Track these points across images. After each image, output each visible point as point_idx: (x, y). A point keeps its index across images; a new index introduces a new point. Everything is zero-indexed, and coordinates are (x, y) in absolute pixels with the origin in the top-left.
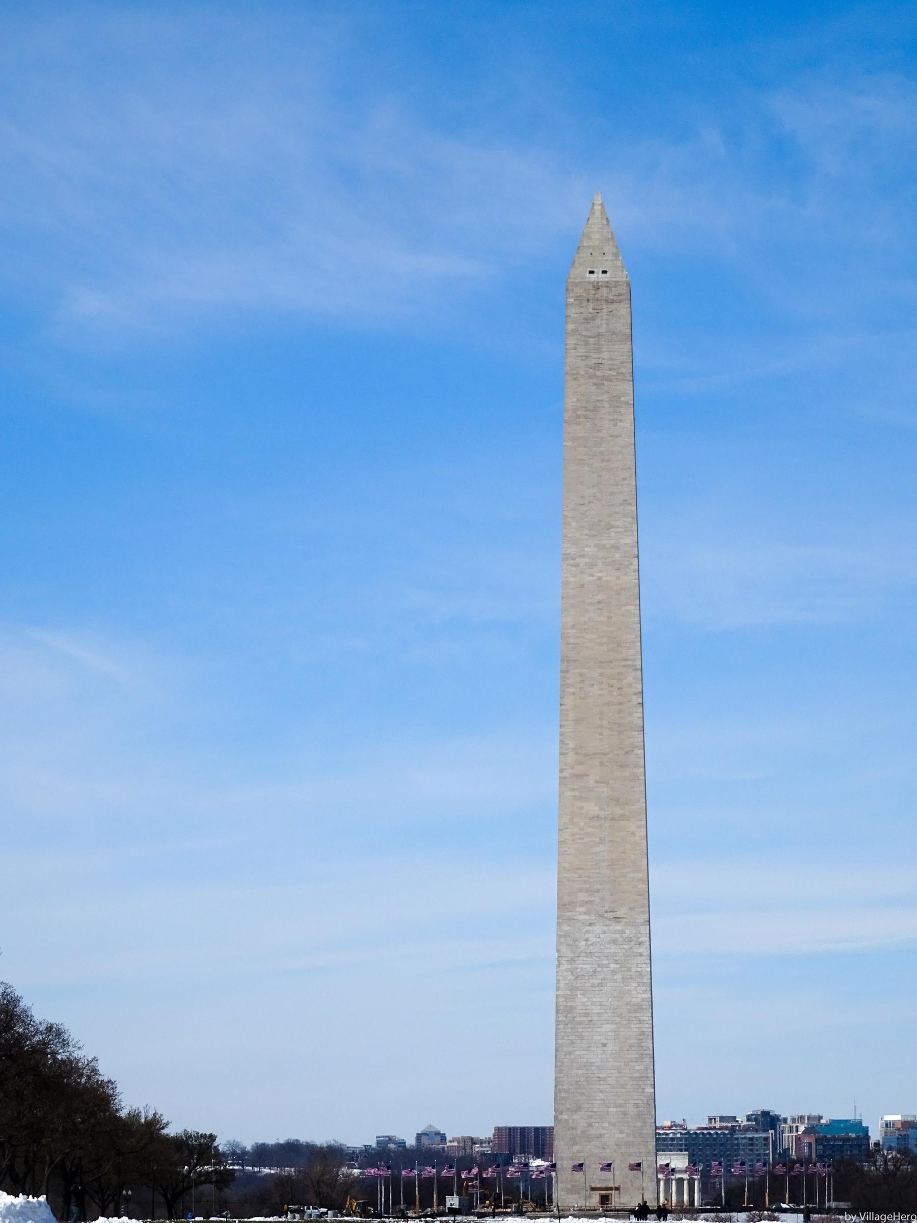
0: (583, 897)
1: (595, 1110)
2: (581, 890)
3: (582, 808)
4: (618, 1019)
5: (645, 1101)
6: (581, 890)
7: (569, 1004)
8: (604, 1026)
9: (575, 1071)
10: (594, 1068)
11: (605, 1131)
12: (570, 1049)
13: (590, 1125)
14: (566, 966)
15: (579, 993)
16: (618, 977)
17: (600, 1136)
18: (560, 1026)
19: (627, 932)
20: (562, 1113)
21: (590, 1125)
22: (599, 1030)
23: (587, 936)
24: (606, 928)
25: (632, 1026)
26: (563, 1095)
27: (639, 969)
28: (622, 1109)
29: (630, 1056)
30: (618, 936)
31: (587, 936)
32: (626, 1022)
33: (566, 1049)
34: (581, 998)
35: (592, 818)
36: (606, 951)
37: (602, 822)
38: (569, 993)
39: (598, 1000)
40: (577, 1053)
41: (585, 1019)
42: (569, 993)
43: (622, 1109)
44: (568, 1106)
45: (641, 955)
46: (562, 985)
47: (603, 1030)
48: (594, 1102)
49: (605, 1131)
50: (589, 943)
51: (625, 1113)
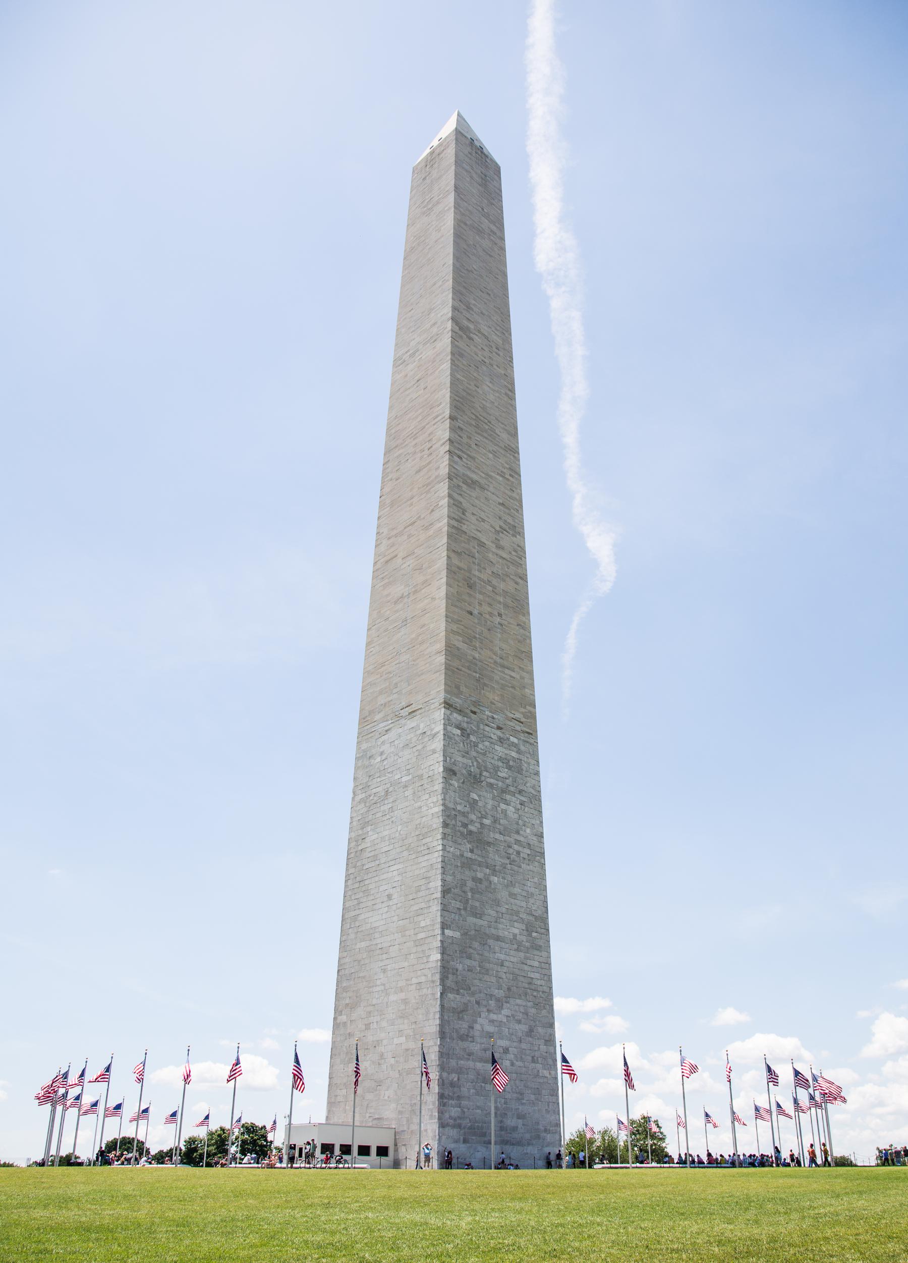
0: (382, 700)
1: (374, 1001)
2: (381, 692)
3: (388, 595)
4: (406, 853)
5: (430, 975)
6: (381, 692)
7: (360, 848)
8: (392, 869)
9: (358, 946)
10: (377, 935)
11: (383, 1035)
12: (357, 912)
13: (368, 1027)
14: (360, 797)
15: (369, 828)
16: (409, 793)
17: (378, 1043)
18: (350, 882)
19: (422, 726)
20: (341, 1013)
21: (368, 1027)
22: (385, 876)
23: (383, 748)
24: (400, 730)
25: (421, 859)
26: (344, 985)
27: (431, 773)
28: (402, 995)
29: (415, 908)
30: (412, 735)
31: (383, 748)
32: (414, 856)
33: (353, 914)
34: (372, 836)
35: (396, 603)
36: (400, 760)
37: (406, 600)
38: (360, 832)
39: (386, 833)
40: (362, 917)
41: (373, 864)
42: (360, 832)
43: (402, 995)
44: (347, 1001)
45: (434, 752)
46: (355, 823)
47: (390, 875)
48: (375, 989)
49: (383, 1035)
50: (384, 757)
51: (405, 1001)
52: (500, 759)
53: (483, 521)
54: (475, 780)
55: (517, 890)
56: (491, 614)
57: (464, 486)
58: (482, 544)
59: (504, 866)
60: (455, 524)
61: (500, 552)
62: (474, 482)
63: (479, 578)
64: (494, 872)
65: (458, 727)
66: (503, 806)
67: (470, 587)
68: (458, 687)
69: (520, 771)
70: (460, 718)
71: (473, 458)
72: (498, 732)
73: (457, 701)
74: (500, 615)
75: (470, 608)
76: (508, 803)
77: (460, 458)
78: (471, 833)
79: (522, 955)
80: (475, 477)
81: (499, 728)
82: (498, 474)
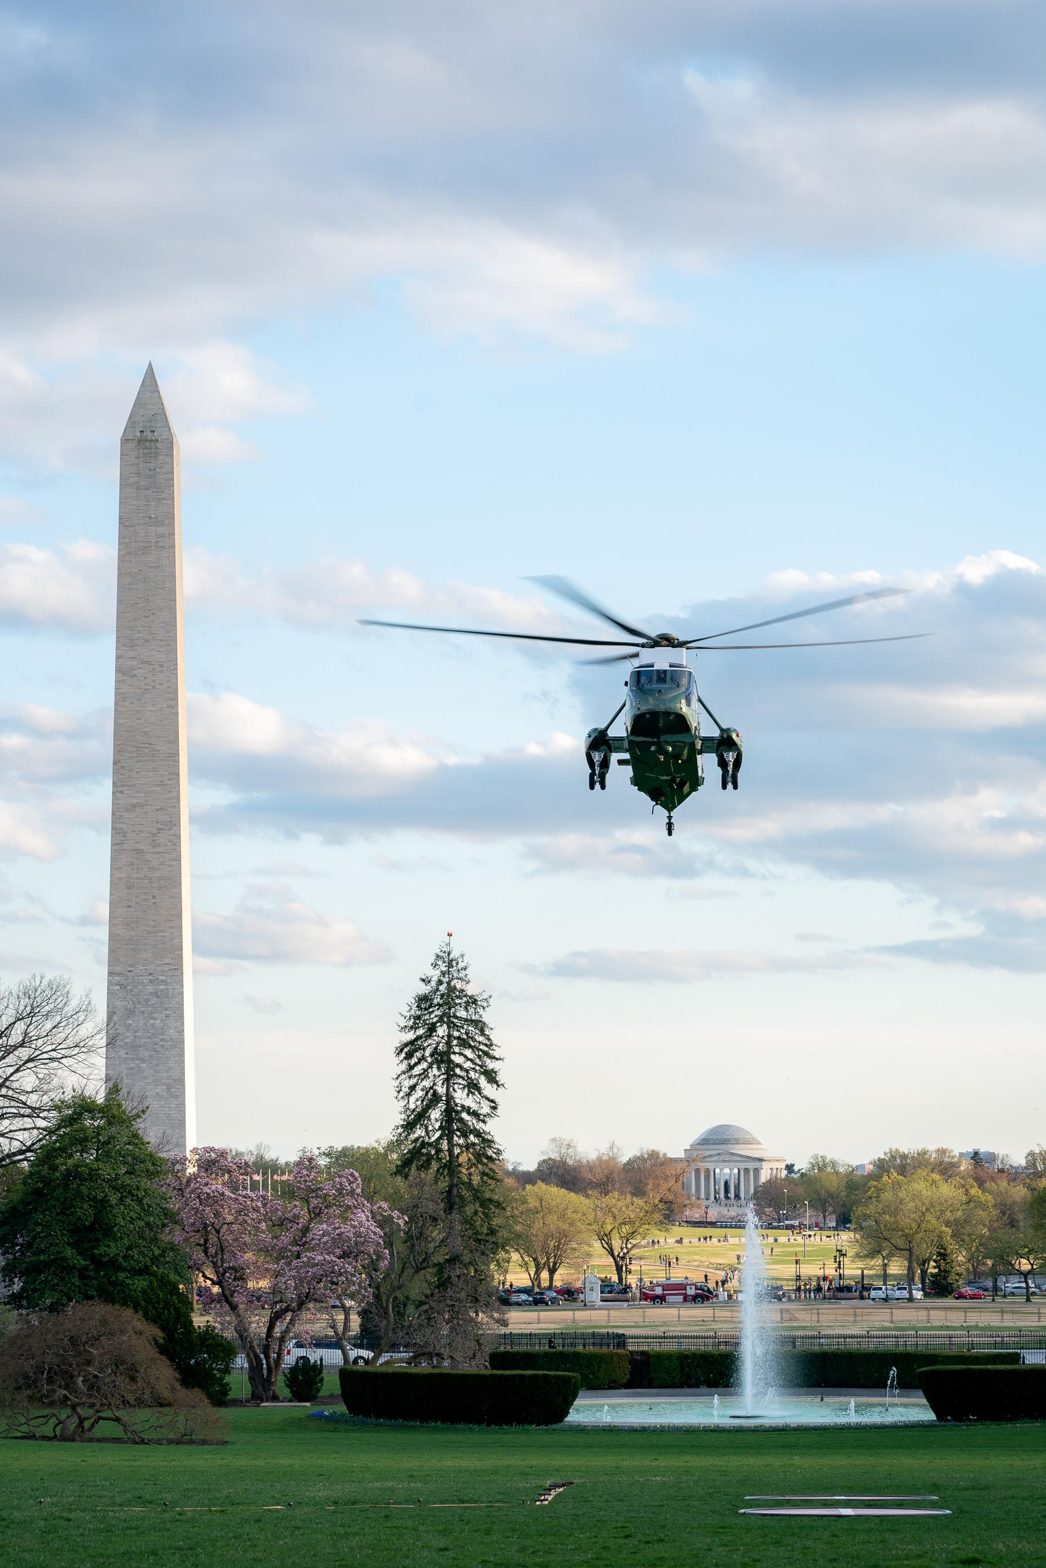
52: (151, 994)
53: (142, 832)
54: (130, 1013)
55: (161, 1067)
56: (146, 900)
57: (125, 815)
58: (140, 852)
59: (151, 1056)
60: (117, 847)
61: (158, 850)
62: (134, 806)
63: (137, 878)
64: (143, 1060)
65: (117, 985)
66: (152, 1022)
67: (129, 888)
68: (118, 960)
69: (167, 996)
70: (119, 978)
71: (134, 786)
72: (150, 977)
73: (118, 969)
74: (154, 897)
75: (129, 903)
76: (154, 1019)
77: (122, 792)
78: (126, 1043)
79: (162, 1103)
80: (135, 801)
81: (150, 974)
82: (157, 786)
